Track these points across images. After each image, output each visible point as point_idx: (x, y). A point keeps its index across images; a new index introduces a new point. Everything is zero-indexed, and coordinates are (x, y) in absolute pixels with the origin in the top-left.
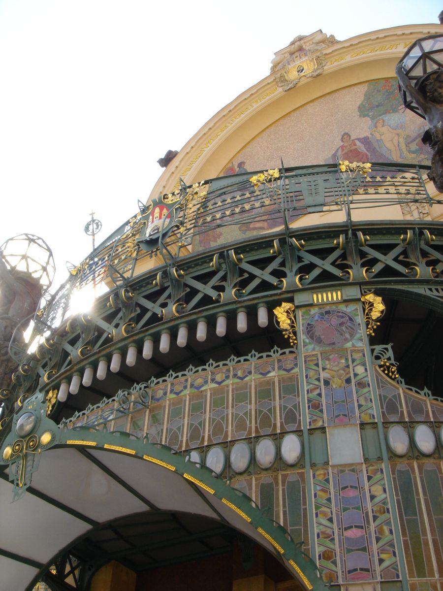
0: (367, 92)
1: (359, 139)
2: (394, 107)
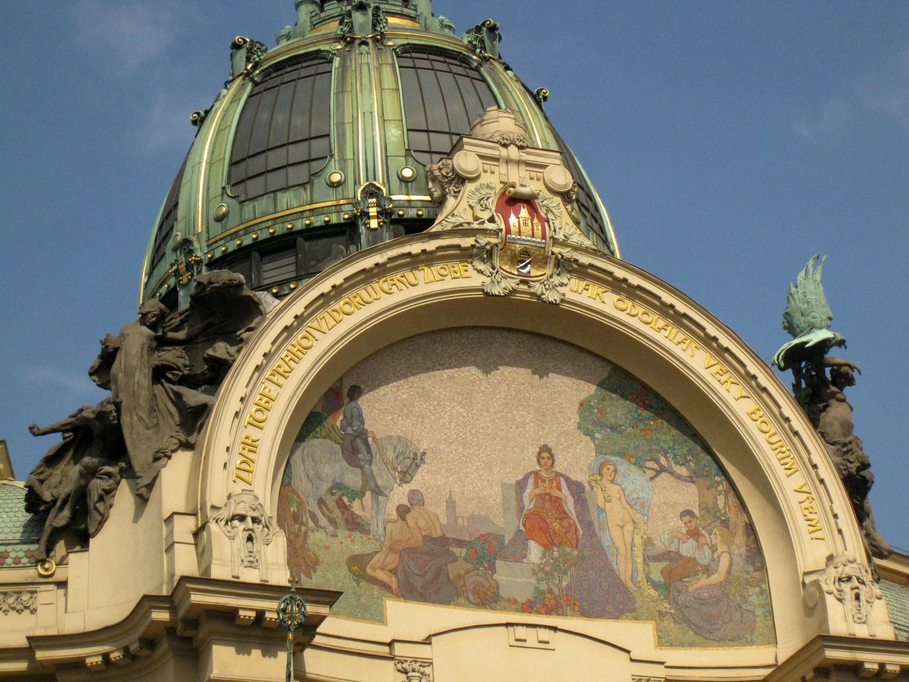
1: (568, 480)
2: (640, 454)
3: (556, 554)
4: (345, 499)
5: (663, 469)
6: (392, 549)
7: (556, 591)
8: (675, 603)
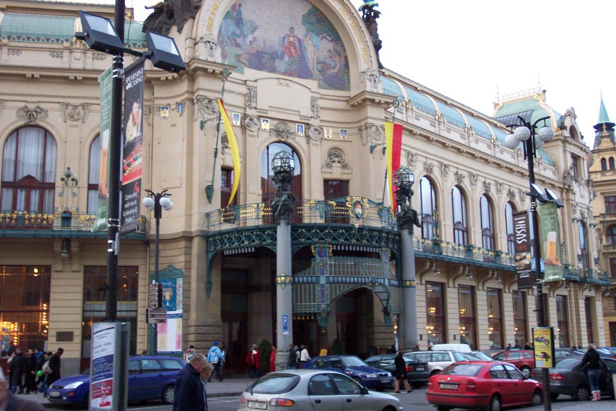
5: (324, 37)
6: (248, 54)
8: (323, 77)
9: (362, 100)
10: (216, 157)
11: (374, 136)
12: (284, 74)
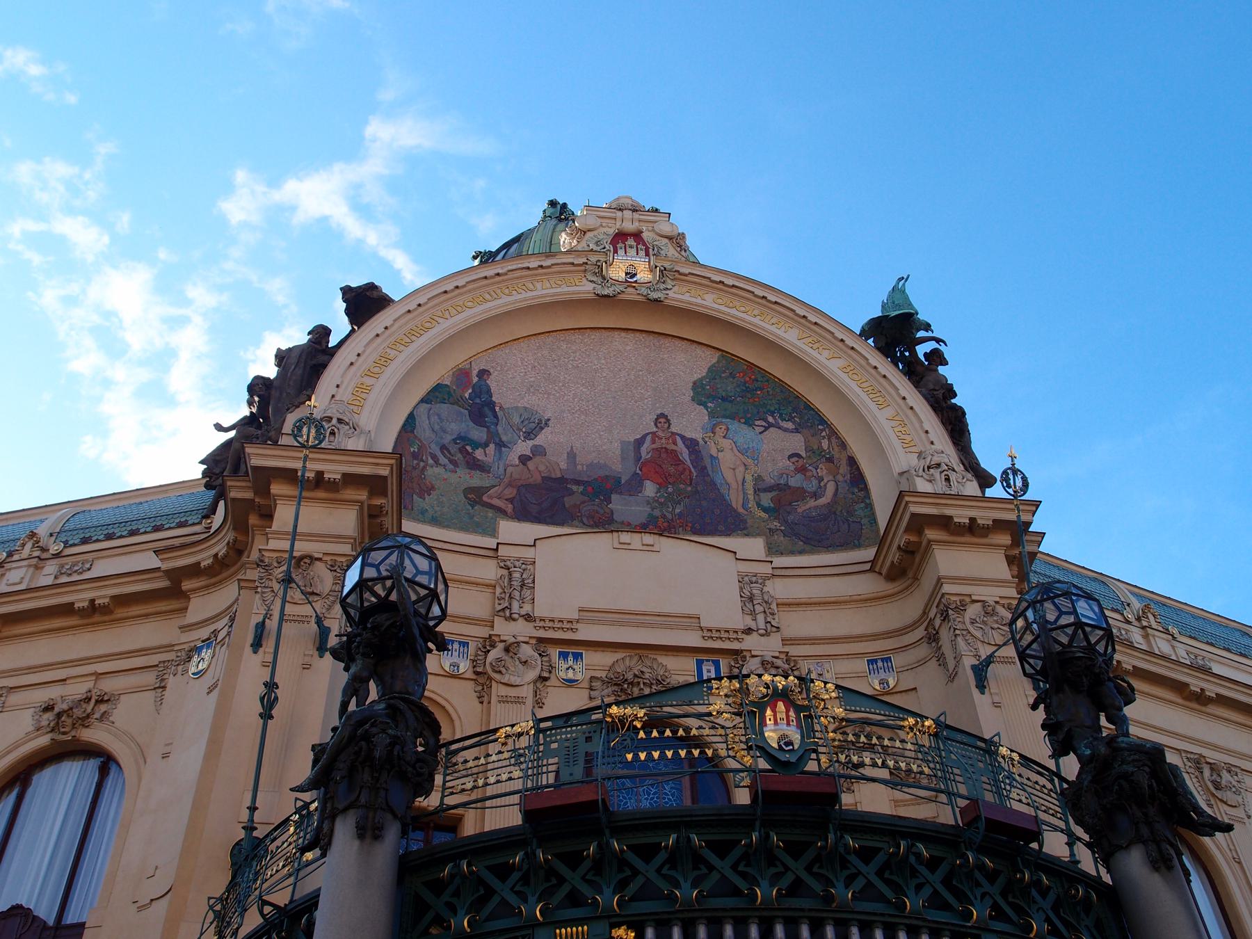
0: (713, 366)
1: (683, 437)
3: (670, 490)
4: (469, 448)
5: (770, 425)
6: (510, 485)
7: (669, 516)
9: (907, 530)
10: (267, 715)
11: (978, 634)
12: (642, 528)
